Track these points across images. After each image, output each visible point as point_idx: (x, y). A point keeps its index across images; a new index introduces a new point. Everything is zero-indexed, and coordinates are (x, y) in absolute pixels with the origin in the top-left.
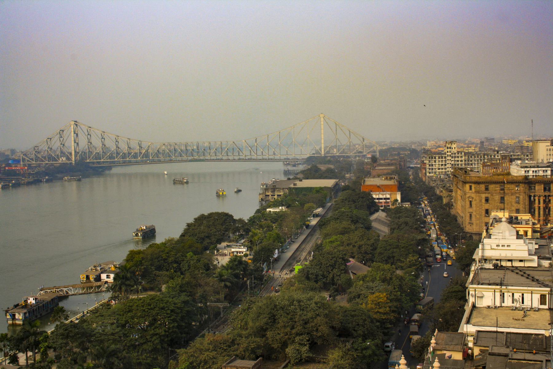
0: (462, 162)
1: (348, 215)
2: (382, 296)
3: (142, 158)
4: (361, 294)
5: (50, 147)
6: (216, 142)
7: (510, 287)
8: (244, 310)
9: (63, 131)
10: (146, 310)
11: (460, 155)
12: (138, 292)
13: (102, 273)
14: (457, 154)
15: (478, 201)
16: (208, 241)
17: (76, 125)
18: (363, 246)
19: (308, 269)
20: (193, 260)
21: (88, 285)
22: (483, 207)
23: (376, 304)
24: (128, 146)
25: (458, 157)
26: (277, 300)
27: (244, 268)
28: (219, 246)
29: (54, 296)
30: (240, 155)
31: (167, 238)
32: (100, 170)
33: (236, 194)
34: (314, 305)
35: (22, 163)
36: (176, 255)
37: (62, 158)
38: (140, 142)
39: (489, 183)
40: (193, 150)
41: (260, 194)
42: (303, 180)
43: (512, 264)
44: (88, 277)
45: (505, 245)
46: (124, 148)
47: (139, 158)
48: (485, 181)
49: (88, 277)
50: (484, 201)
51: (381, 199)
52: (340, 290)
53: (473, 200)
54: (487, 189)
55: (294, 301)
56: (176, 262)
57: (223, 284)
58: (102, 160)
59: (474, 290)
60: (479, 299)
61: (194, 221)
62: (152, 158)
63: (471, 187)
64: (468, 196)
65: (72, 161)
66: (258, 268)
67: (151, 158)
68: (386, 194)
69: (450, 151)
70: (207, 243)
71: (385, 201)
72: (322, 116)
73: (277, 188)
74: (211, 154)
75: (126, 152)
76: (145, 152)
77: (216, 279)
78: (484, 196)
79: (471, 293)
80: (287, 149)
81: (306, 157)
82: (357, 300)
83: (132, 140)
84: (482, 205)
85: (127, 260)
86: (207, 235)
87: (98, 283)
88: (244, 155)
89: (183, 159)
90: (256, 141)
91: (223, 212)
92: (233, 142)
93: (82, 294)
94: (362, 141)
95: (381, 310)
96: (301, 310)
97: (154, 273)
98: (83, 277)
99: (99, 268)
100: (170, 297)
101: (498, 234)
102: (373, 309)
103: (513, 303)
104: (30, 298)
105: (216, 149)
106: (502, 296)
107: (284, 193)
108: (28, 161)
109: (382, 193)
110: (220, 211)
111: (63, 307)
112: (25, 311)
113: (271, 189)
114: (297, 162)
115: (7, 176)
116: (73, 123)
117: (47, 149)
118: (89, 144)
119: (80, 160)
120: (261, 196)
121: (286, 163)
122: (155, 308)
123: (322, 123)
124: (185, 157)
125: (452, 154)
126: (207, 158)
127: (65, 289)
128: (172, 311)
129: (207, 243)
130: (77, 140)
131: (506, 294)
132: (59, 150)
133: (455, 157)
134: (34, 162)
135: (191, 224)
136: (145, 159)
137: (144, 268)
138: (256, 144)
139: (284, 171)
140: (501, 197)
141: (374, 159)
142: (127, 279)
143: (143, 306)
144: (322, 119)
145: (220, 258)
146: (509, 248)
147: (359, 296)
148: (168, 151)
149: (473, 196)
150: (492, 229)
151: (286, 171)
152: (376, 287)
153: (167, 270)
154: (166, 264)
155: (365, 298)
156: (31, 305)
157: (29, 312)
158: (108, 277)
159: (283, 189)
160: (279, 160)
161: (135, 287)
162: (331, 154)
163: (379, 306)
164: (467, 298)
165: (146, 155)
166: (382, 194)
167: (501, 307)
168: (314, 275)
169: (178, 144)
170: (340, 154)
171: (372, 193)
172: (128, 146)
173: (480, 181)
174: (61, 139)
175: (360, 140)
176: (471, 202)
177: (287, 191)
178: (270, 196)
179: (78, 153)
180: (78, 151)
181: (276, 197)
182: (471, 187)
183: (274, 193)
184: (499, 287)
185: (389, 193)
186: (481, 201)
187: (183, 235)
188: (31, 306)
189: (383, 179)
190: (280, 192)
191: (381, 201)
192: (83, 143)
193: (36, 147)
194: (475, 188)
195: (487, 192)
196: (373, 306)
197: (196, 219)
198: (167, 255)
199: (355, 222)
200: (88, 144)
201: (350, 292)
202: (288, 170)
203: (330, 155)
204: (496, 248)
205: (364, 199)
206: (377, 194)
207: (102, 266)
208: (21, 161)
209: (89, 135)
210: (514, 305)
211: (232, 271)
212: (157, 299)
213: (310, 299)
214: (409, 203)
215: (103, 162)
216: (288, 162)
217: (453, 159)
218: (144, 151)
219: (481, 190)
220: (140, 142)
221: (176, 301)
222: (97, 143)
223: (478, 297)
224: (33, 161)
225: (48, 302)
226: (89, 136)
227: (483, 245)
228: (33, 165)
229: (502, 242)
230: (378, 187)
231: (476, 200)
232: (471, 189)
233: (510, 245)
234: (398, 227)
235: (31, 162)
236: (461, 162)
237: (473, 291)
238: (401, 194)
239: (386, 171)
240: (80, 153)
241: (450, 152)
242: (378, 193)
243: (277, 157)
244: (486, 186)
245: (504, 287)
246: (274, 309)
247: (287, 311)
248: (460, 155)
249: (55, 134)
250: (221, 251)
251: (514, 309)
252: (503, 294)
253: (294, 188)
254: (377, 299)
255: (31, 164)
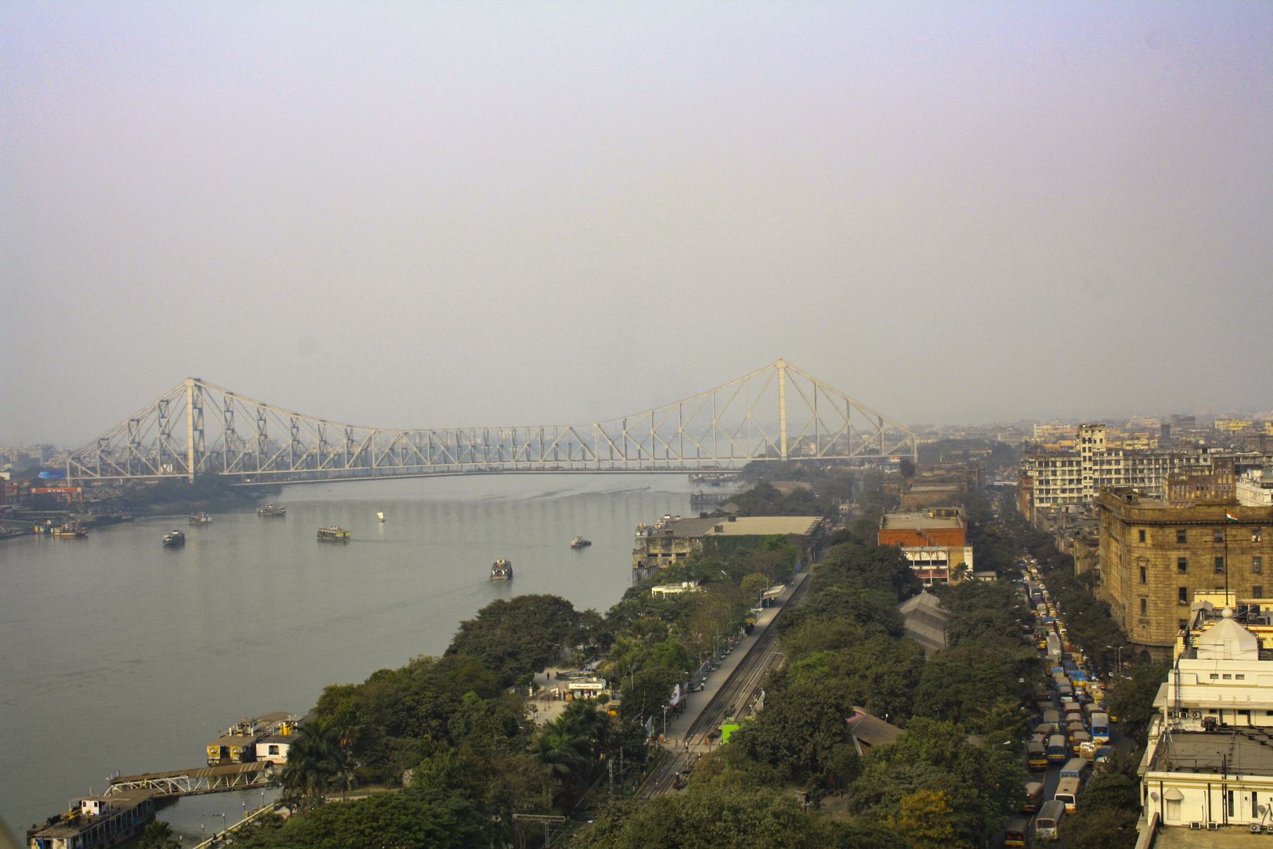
0: (1120, 473)
1: (847, 602)
2: (933, 797)
3: (355, 466)
4: (884, 794)
5: (137, 440)
6: (528, 428)
7: (1246, 778)
8: (603, 832)
9: (168, 402)
10: (367, 831)
11: (1113, 457)
12: (345, 788)
13: (259, 741)
14: (1106, 455)
15: (1160, 567)
16: (512, 664)
17: (200, 388)
18: (886, 677)
19: (753, 732)
20: (478, 710)
21: (227, 769)
22: (1174, 582)
23: (919, 818)
24: (321, 437)
25: (1109, 462)
26: (683, 807)
27: (598, 729)
28: (538, 676)
29: (144, 797)
30: (587, 458)
31: (415, 658)
32: (255, 494)
33: (574, 550)
34: (770, 819)
35: (68, 478)
36: (436, 698)
37: (165, 466)
38: (349, 429)
39: (1186, 524)
40: (474, 447)
41: (635, 552)
42: (737, 519)
43: (1249, 721)
44: (224, 752)
45: (1230, 675)
46: (310, 441)
47: (347, 467)
48: (1176, 519)
49: (224, 752)
50: (1174, 567)
51: (927, 563)
52: (831, 784)
53: (1150, 566)
54: (1182, 539)
55: (722, 810)
56: (436, 715)
57: (549, 769)
58: (259, 471)
59: (1159, 783)
60: (1171, 805)
61: (478, 617)
62: (378, 466)
63: (1142, 534)
64: (1137, 555)
65: (187, 472)
66: (634, 730)
67: (374, 466)
68: (937, 552)
69: (1090, 448)
70: (511, 669)
71: (934, 568)
72: (781, 365)
73: (675, 538)
74: (517, 457)
75: (316, 451)
76: (361, 453)
77: (533, 756)
78: (1174, 555)
79: (1150, 790)
80: (698, 445)
81: (744, 464)
82: (875, 808)
84: (1170, 577)
85: (320, 711)
86: (510, 650)
87: (251, 767)
88: (596, 460)
89: (450, 469)
90: (625, 426)
91: (547, 594)
93: (211, 792)
94: (878, 425)
95: (931, 833)
96: (739, 831)
97: (384, 741)
98: (213, 752)
99: (251, 731)
100: (422, 800)
101: (1213, 648)
102: (913, 830)
103: (1255, 815)
104: (88, 803)
105: (529, 445)
106: (1229, 798)
107: (693, 550)
108: (84, 473)
109: (927, 548)
110: (541, 592)
111: (167, 824)
112: (75, 833)
113: (663, 539)
114: (723, 474)
115: (35, 510)
116: (192, 383)
117: (129, 445)
118: (229, 432)
119: (207, 470)
120: (638, 557)
121: (695, 478)
122: (387, 825)
123: (782, 382)
124: (457, 463)
125: (1095, 454)
126: (507, 465)
127: (170, 781)
128: (429, 833)
129: (511, 669)
130: (201, 423)
131: (1236, 794)
132: (158, 447)
133: (1102, 463)
134: (98, 476)
135: (473, 624)
136: (360, 468)
137: (361, 730)
138: (624, 433)
139: (692, 495)
140: (1217, 559)
141: (907, 468)
142: (320, 756)
143: (359, 822)
144: (782, 373)
145: (540, 706)
146: (1239, 682)
147: (878, 798)
148: (415, 449)
149: (1148, 556)
150: (1198, 636)
151: (696, 496)
152: (919, 776)
153: (416, 735)
154: (414, 720)
155: (893, 802)
156: (91, 819)
157: (84, 835)
158: (273, 750)
159: (691, 539)
160: (681, 470)
161: (340, 774)
162: (804, 456)
163: (927, 822)
164: (1142, 804)
165: (364, 459)
166: (928, 552)
167: (1226, 825)
168: (767, 747)
169: (438, 432)
170: (824, 455)
171: (903, 549)
172: (321, 437)
173: (1166, 519)
174: (164, 421)
175: (873, 423)
176: (1143, 570)
177: (699, 544)
178: (660, 556)
179: (203, 454)
180: (201, 449)
181: (673, 558)
182: (1142, 534)
183: (669, 550)
184: (1219, 777)
185: (945, 548)
186: (1167, 567)
187: (452, 651)
188: (89, 820)
189: (931, 514)
190: (684, 547)
191: (925, 568)
192: (215, 433)
193: (103, 439)
194: (1152, 536)
195: (1182, 545)
196: (912, 821)
197: (483, 612)
198: (417, 697)
199: (864, 618)
200: (226, 434)
201: (857, 789)
202: (702, 495)
203: (801, 458)
204: (1211, 681)
205: (885, 564)
206: (916, 552)
207: (259, 726)
208: (68, 474)
209: (228, 411)
210: (1258, 820)
211: (571, 737)
212: (393, 803)
213: (761, 805)
214: (993, 574)
215: (263, 477)
216: (700, 476)
217: (1097, 467)
218: (359, 450)
219: (1168, 543)
220: (349, 429)
221: (439, 810)
222: (247, 430)
223: (1168, 801)
224: (96, 473)
225: (129, 812)
226: (229, 414)
227: (1178, 674)
228: (95, 484)
229: (1223, 667)
230: (919, 534)
231: (1155, 566)
232: (1142, 538)
233: (1243, 676)
234: (969, 631)
235: (92, 476)
236: (1116, 473)
237: (1156, 786)
238: (974, 552)
239: (936, 497)
240: (208, 454)
241: (1090, 451)
242: (918, 549)
243: (673, 464)
244: (1179, 532)
245: (1231, 778)
246: (674, 830)
247: (707, 833)
248: (1113, 457)
249: (150, 410)
250: (542, 688)
251: (1258, 830)
252: (1231, 793)
253: (715, 537)
254: (921, 805)
255: (90, 480)
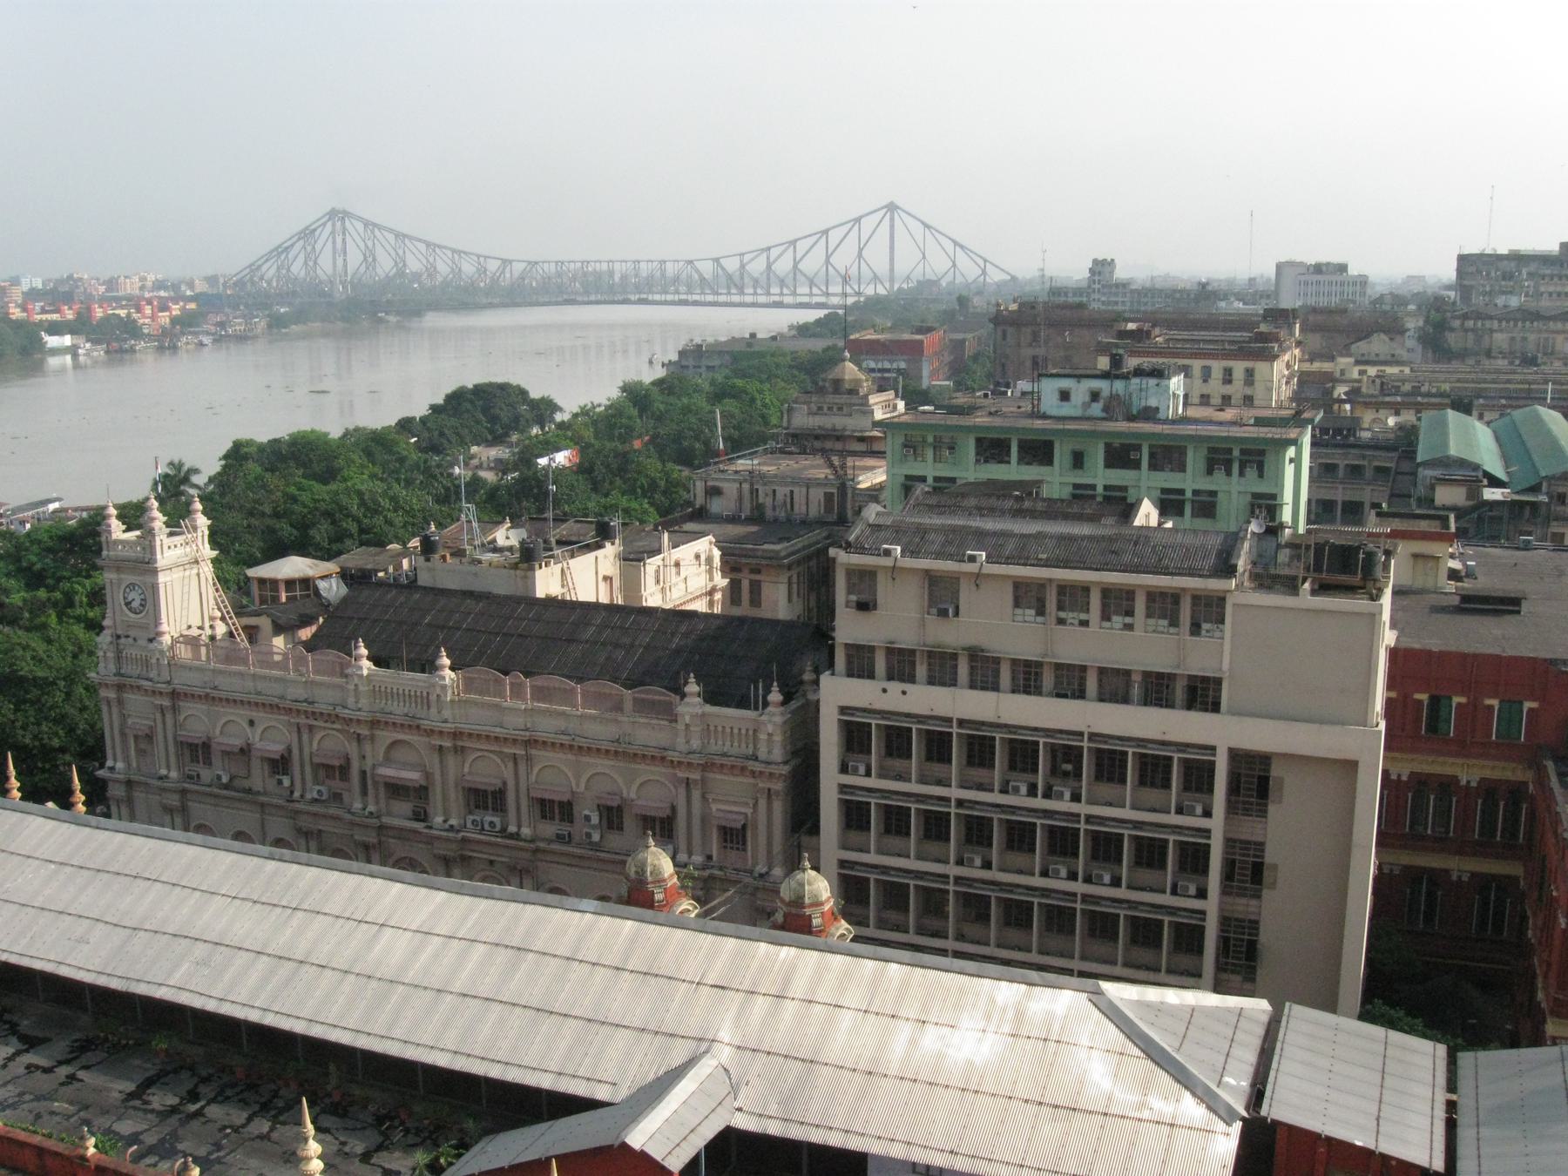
50: (1028, 363)
51: (888, 371)
83: (465, 253)
92: (691, 262)
113: (693, 351)
166: (889, 361)
176: (1003, 366)
185: (905, 357)
191: (886, 375)
192: (385, 266)
232: (1004, 338)
